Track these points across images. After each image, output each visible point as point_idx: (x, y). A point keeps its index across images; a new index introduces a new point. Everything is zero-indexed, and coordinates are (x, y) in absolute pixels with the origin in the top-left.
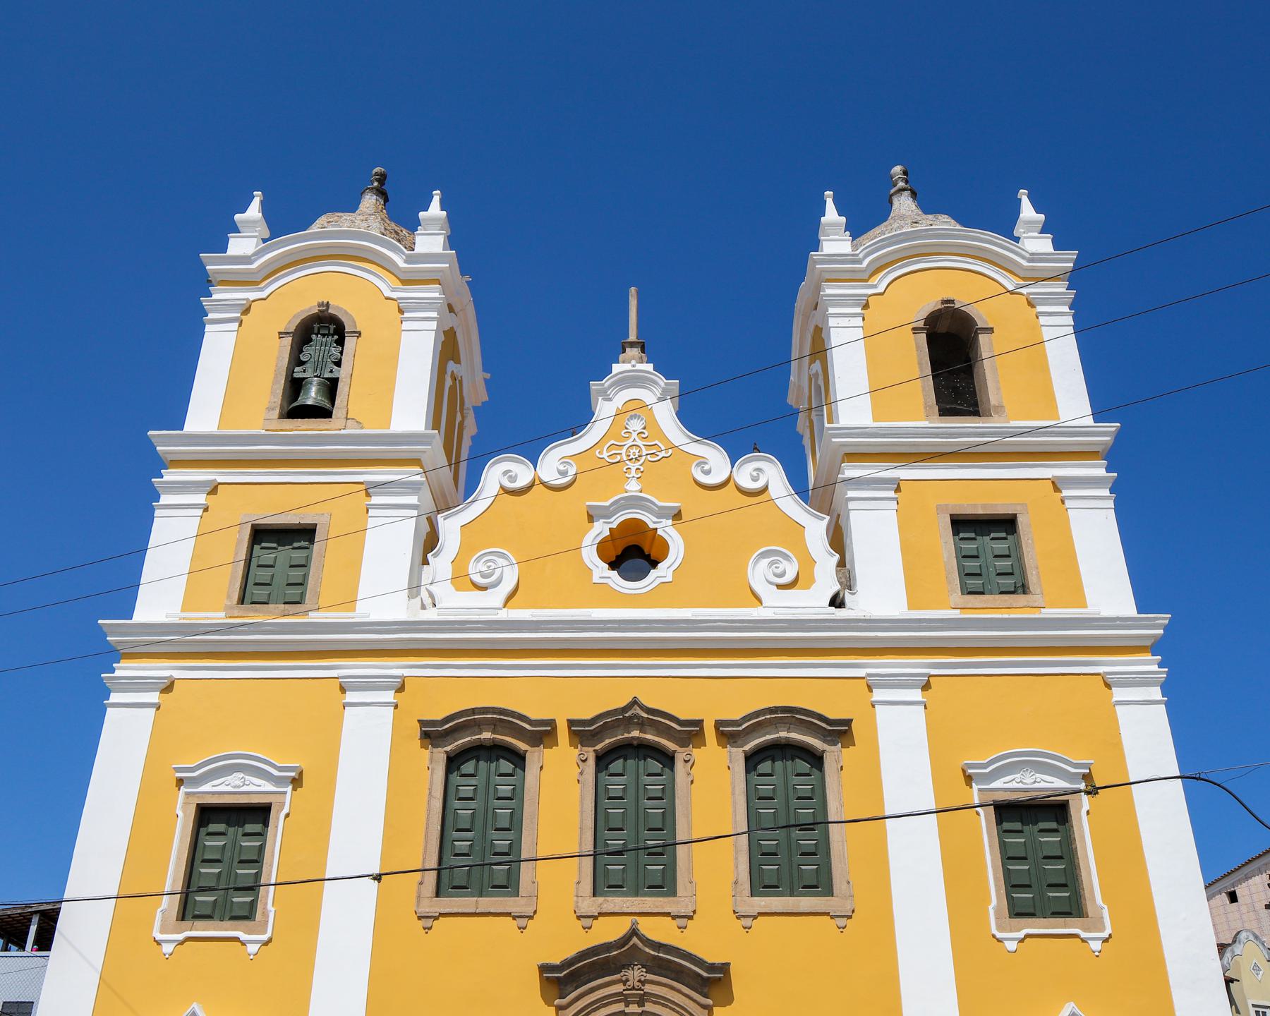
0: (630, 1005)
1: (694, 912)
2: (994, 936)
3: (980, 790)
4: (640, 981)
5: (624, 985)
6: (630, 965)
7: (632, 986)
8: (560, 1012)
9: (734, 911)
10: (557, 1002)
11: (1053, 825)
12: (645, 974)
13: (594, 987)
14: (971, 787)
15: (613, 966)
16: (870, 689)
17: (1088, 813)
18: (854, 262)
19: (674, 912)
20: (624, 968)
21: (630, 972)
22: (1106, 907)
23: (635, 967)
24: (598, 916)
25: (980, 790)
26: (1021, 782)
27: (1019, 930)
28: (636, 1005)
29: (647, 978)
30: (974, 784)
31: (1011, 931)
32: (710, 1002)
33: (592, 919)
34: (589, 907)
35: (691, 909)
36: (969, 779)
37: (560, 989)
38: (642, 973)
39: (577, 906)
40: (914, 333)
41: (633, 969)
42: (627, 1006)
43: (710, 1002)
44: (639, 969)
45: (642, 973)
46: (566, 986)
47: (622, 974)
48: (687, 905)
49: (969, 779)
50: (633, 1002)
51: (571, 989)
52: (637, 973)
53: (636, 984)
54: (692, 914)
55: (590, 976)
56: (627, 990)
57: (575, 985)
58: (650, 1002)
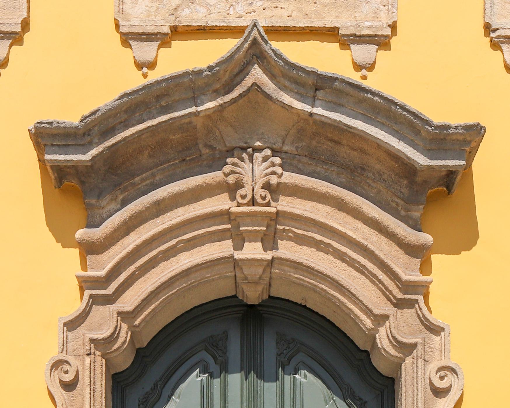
0: (246, 244)
1: (393, 27)
4: (267, 186)
5: (233, 198)
6: (244, 149)
7: (249, 197)
8: (89, 257)
9: (488, 28)
10: (81, 233)
12: (279, 170)
13: (164, 199)
15: (205, 151)
19: (347, 28)
20: (232, 156)
21: (247, 166)
23: (256, 154)
24: (171, 39)
28: (259, 244)
29: (283, 180)
32: (426, 238)
33: (156, 44)
34: (148, 16)
35: (385, 19)
37: (88, 207)
38: (272, 169)
39: (121, 11)
41: (251, 159)
42: (238, 247)
43: (426, 238)
44: (265, 159)
45: (272, 169)
46: (100, 196)
47: (227, 169)
48: (376, 16)
50: (253, 237)
51: (113, 206)
52: (260, 168)
53: (260, 192)
54: (388, 32)
55: (153, 176)
56: (239, 205)
57: (121, 197)
58: (290, 239)
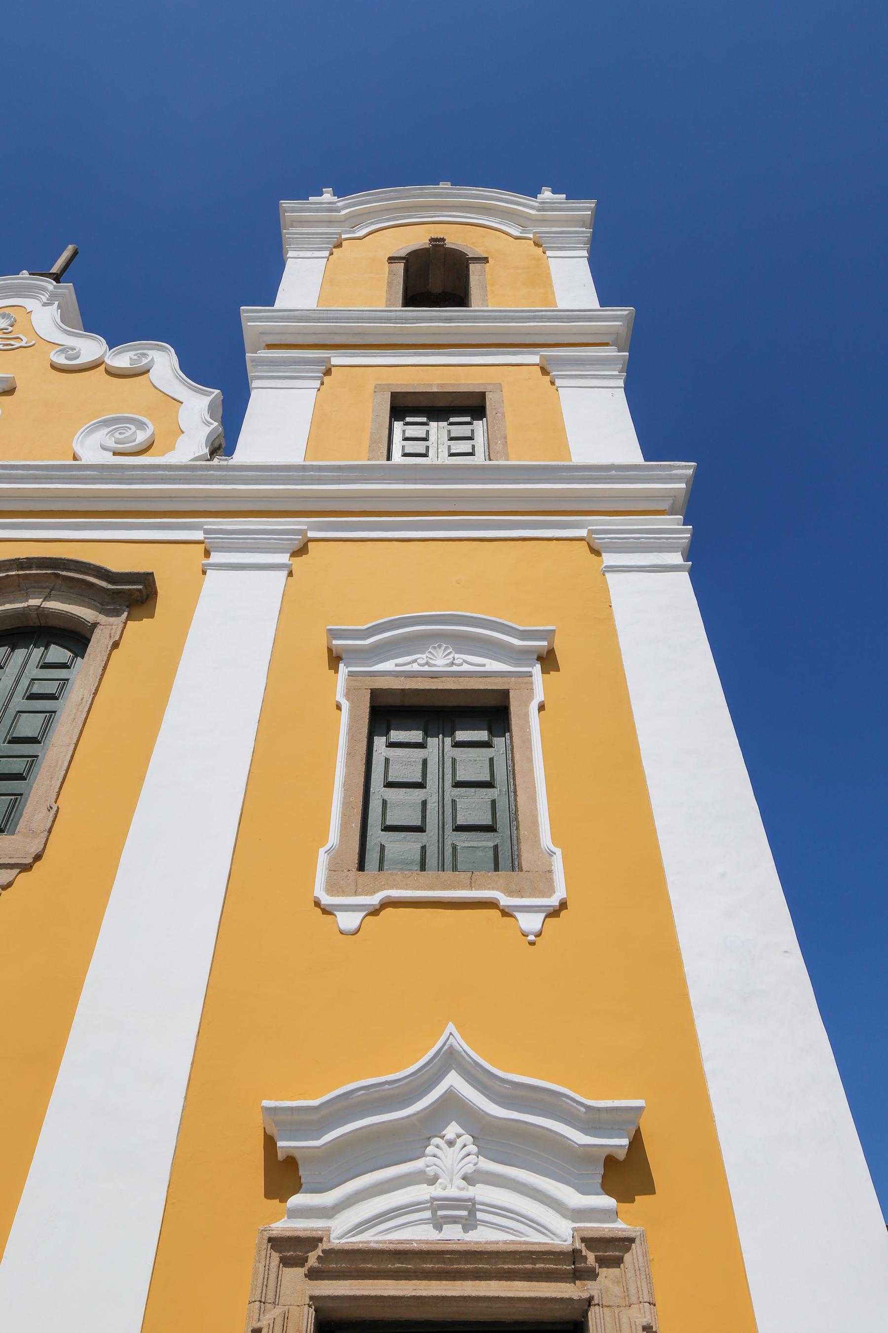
2: (317, 904)
3: (351, 674)
11: (482, 735)
14: (337, 672)
16: (207, 554)
17: (541, 708)
18: (330, 210)
22: (558, 851)
25: (351, 674)
26: (427, 663)
27: (373, 892)
30: (341, 665)
31: (356, 894)
36: (335, 659)
40: (389, 263)
49: (335, 659)
